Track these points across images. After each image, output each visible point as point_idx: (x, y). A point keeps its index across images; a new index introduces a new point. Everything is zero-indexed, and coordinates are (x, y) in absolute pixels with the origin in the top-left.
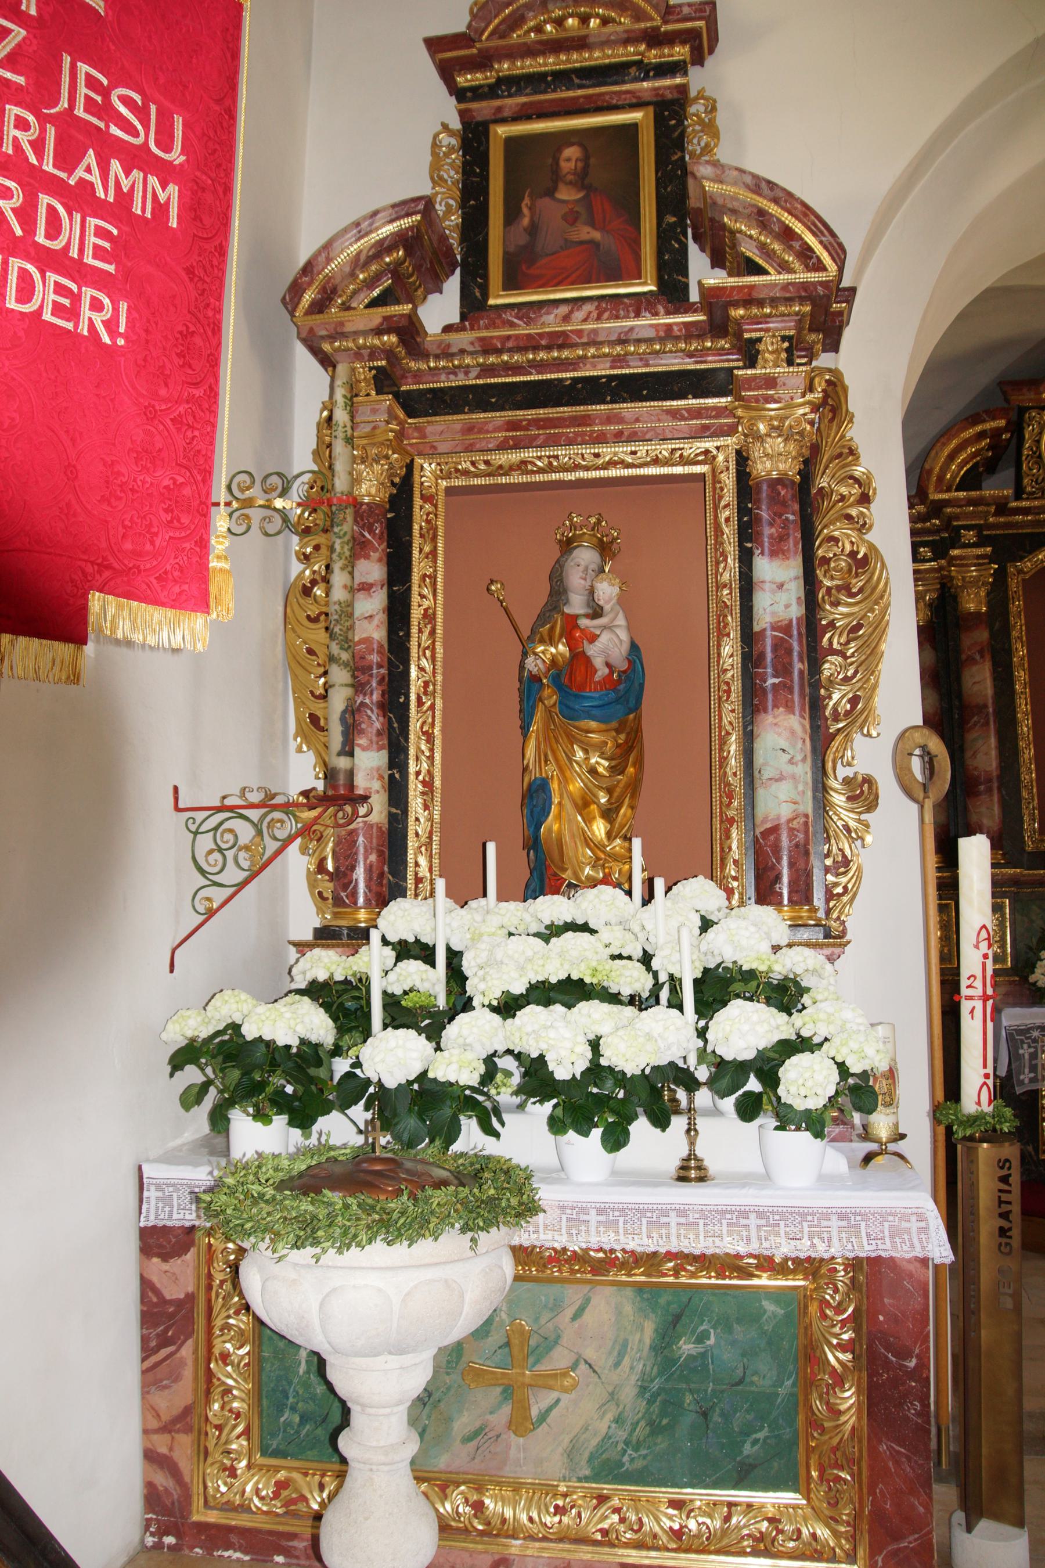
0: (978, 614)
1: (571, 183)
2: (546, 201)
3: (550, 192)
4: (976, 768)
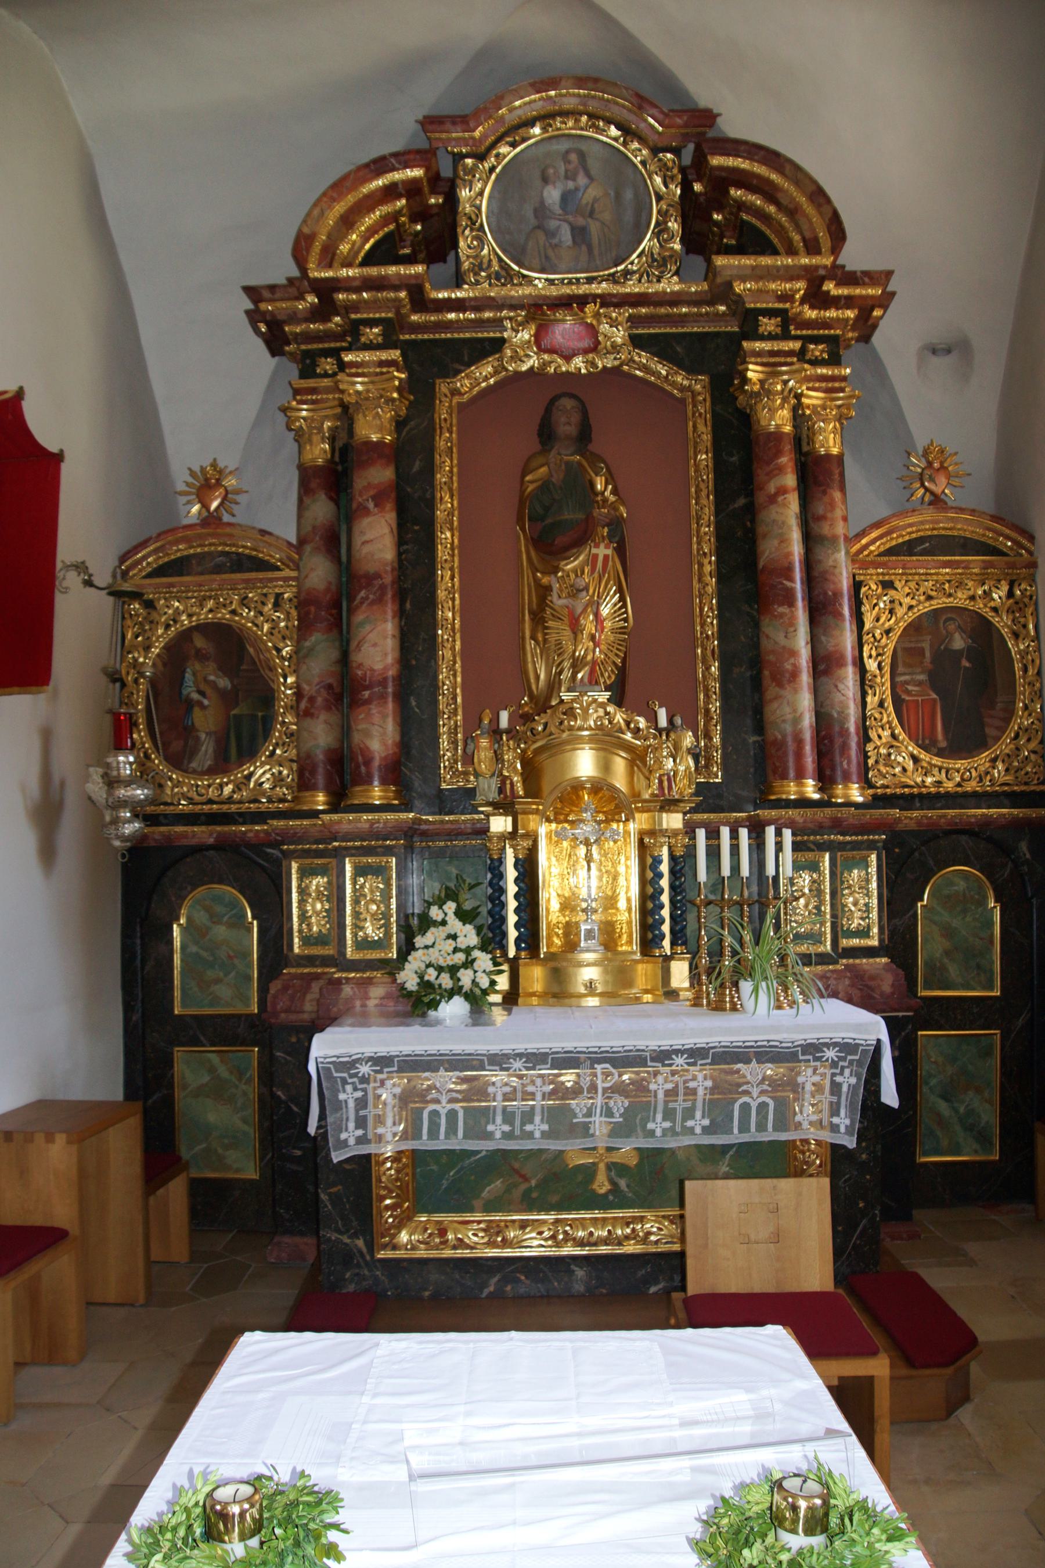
0: (381, 443)
4: (360, 666)
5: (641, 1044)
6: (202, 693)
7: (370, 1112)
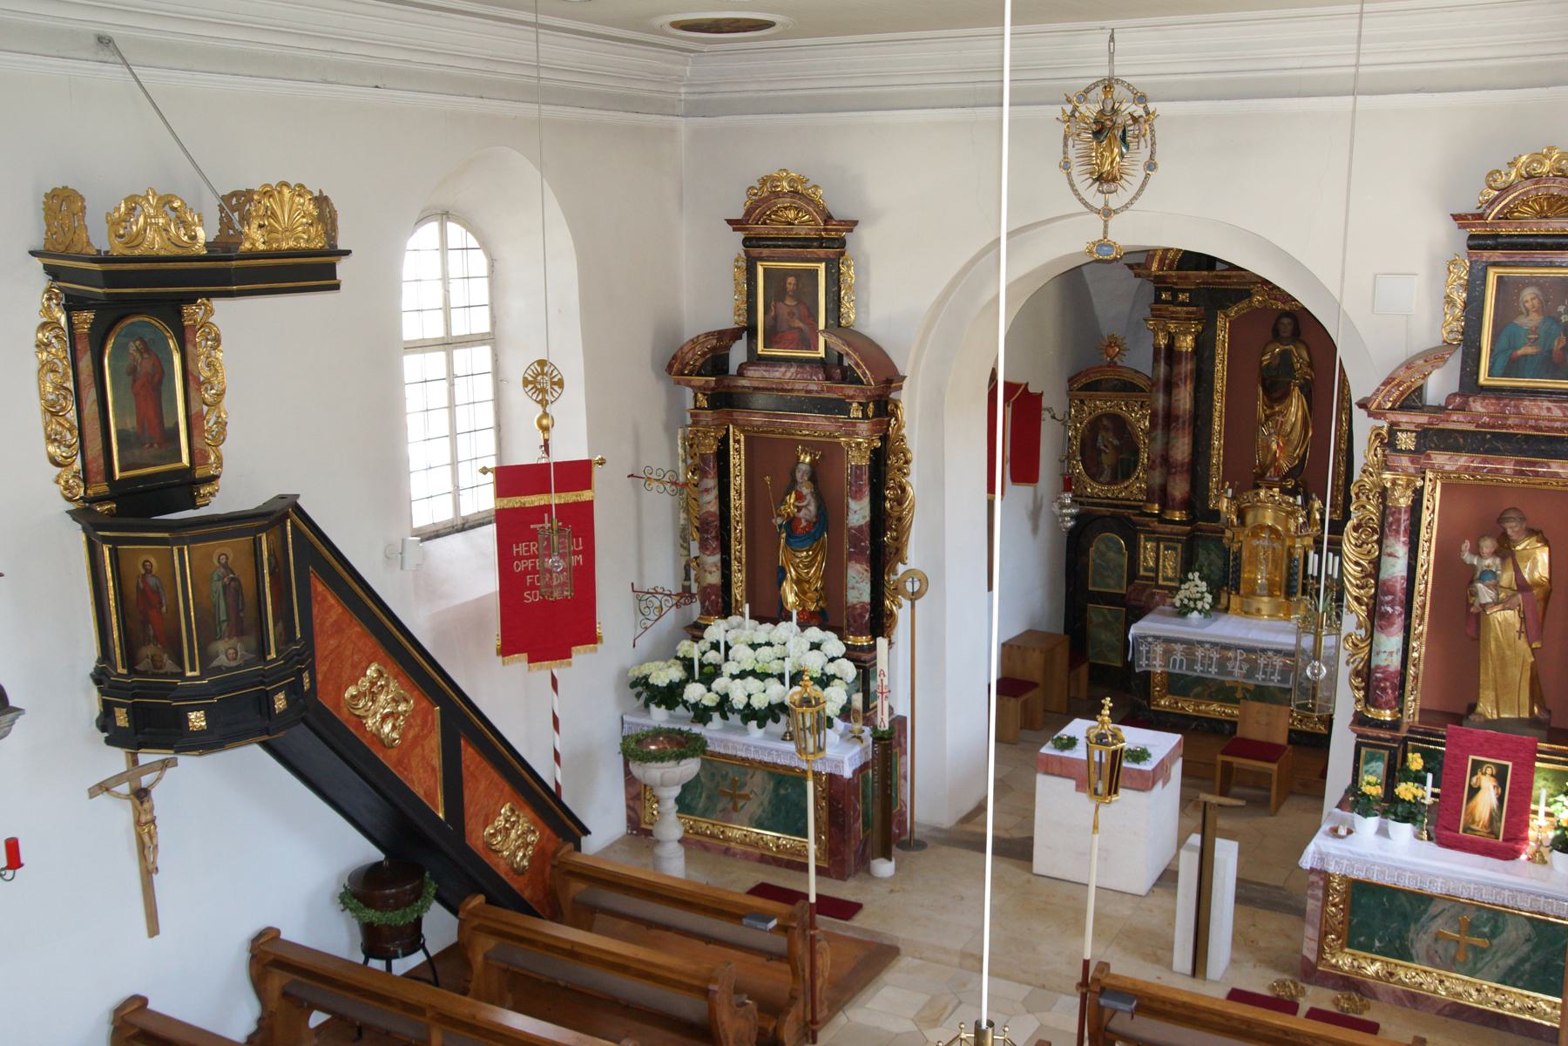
1: (791, 296)
2: (780, 305)
3: (783, 300)
5: (1256, 645)
6: (1105, 446)
7: (1151, 655)
